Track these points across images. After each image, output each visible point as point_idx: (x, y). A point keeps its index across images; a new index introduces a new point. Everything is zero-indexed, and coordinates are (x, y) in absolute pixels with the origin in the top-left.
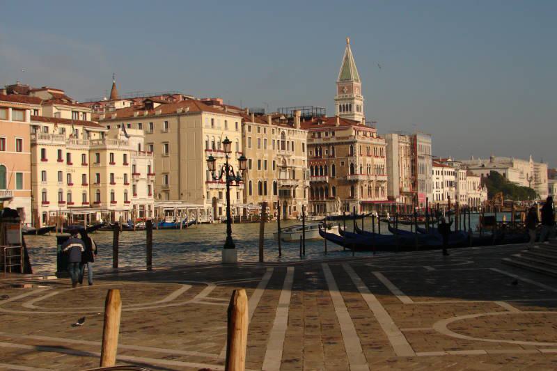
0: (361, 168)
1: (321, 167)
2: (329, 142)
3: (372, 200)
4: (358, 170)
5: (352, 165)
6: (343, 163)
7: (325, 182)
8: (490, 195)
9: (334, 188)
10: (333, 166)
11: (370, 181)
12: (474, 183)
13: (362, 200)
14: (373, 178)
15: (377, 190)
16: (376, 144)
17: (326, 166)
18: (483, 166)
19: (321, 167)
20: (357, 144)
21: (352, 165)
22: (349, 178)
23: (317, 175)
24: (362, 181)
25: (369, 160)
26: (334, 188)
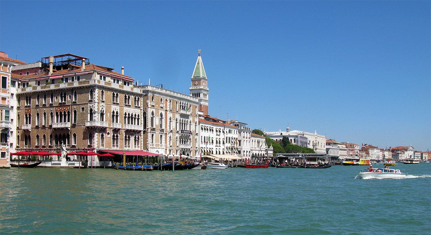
0: (102, 114)
1: (65, 113)
2: (73, 86)
3: (118, 149)
4: (97, 116)
5: (91, 110)
6: (83, 109)
7: (67, 128)
8: (275, 152)
9: (75, 135)
10: (75, 112)
11: (116, 131)
12: (258, 142)
13: (101, 148)
14: (118, 126)
15: (127, 139)
16: (128, 93)
17: (69, 112)
18: (281, 134)
19: (65, 113)
20: (97, 90)
21: (91, 110)
22: (88, 124)
23: (61, 121)
24: (103, 130)
25: (115, 108)
26: (75, 135)
